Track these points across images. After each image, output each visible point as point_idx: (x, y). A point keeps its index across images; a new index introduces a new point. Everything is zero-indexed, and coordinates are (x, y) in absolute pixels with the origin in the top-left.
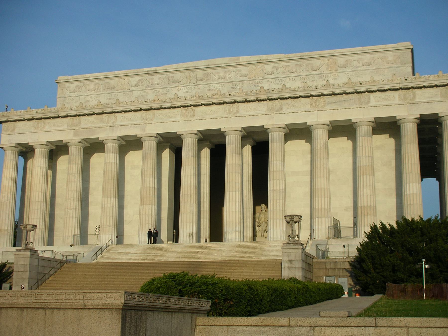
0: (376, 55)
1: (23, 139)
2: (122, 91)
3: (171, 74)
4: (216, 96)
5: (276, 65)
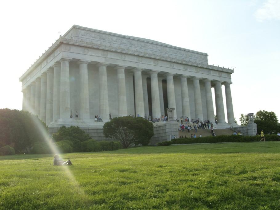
0: (199, 55)
2: (109, 42)
3: (131, 41)
4: (167, 58)
5: (170, 49)
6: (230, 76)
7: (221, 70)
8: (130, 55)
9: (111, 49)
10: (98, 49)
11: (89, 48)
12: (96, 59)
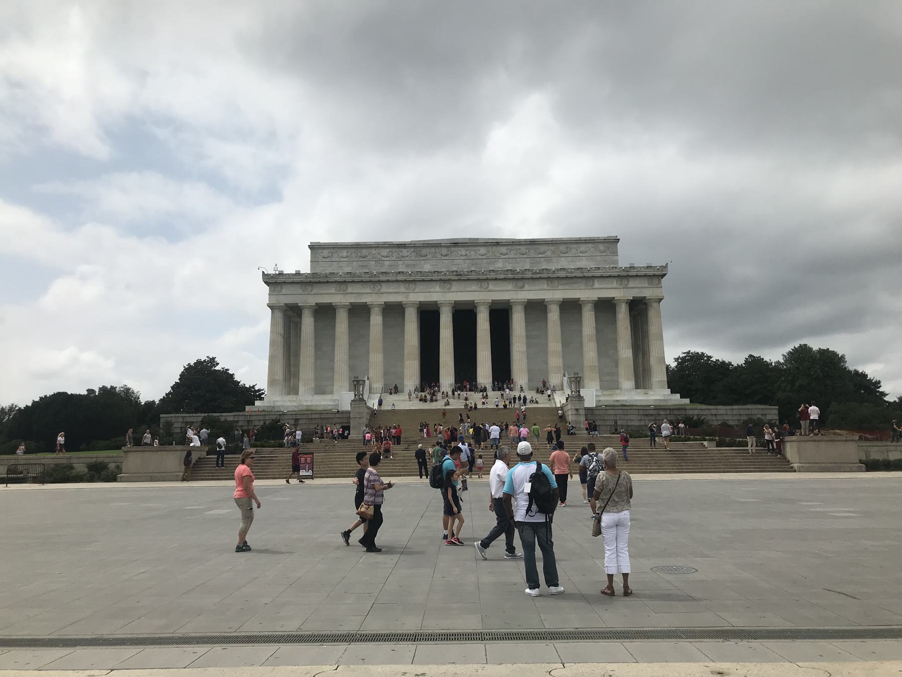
0: (590, 245)
1: (290, 300)
6: (660, 281)
7: (624, 274)
8: (388, 281)
9: (350, 279)
10: (328, 282)
11: (310, 283)
12: (325, 300)
